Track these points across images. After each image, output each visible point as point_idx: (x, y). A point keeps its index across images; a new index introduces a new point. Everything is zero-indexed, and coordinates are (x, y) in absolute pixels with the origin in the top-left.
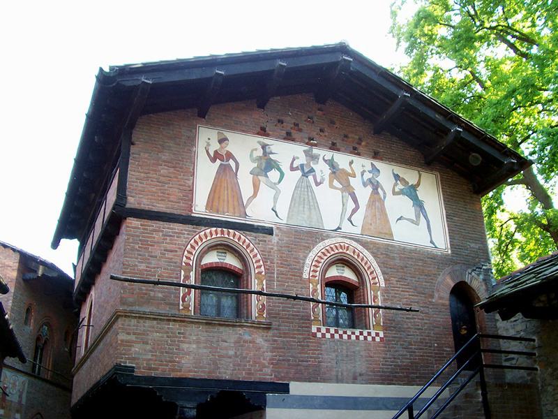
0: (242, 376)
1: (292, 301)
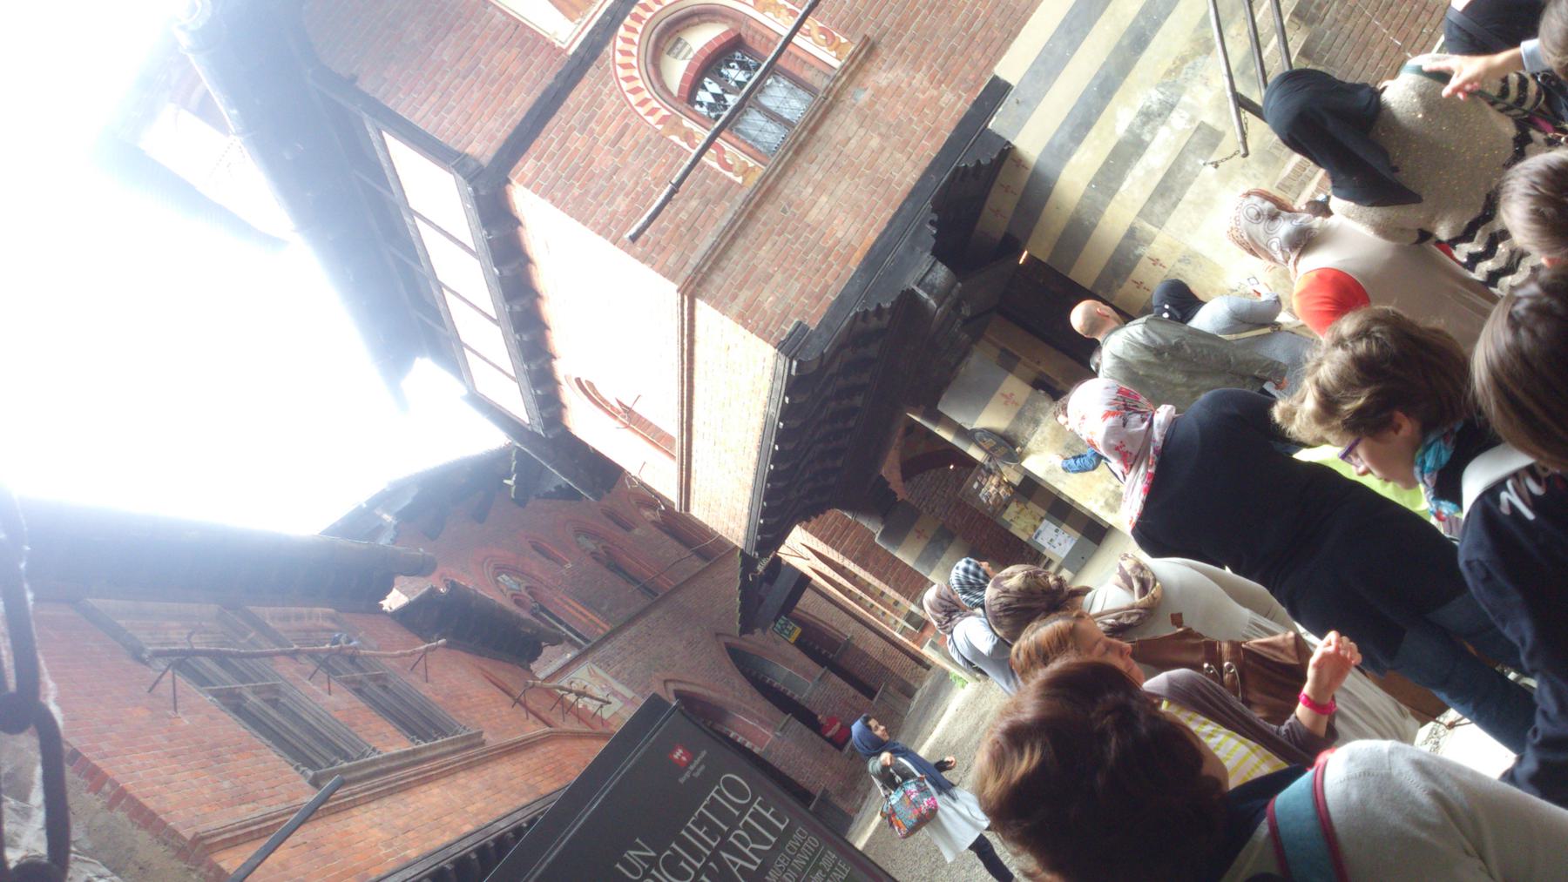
0: (930, 149)
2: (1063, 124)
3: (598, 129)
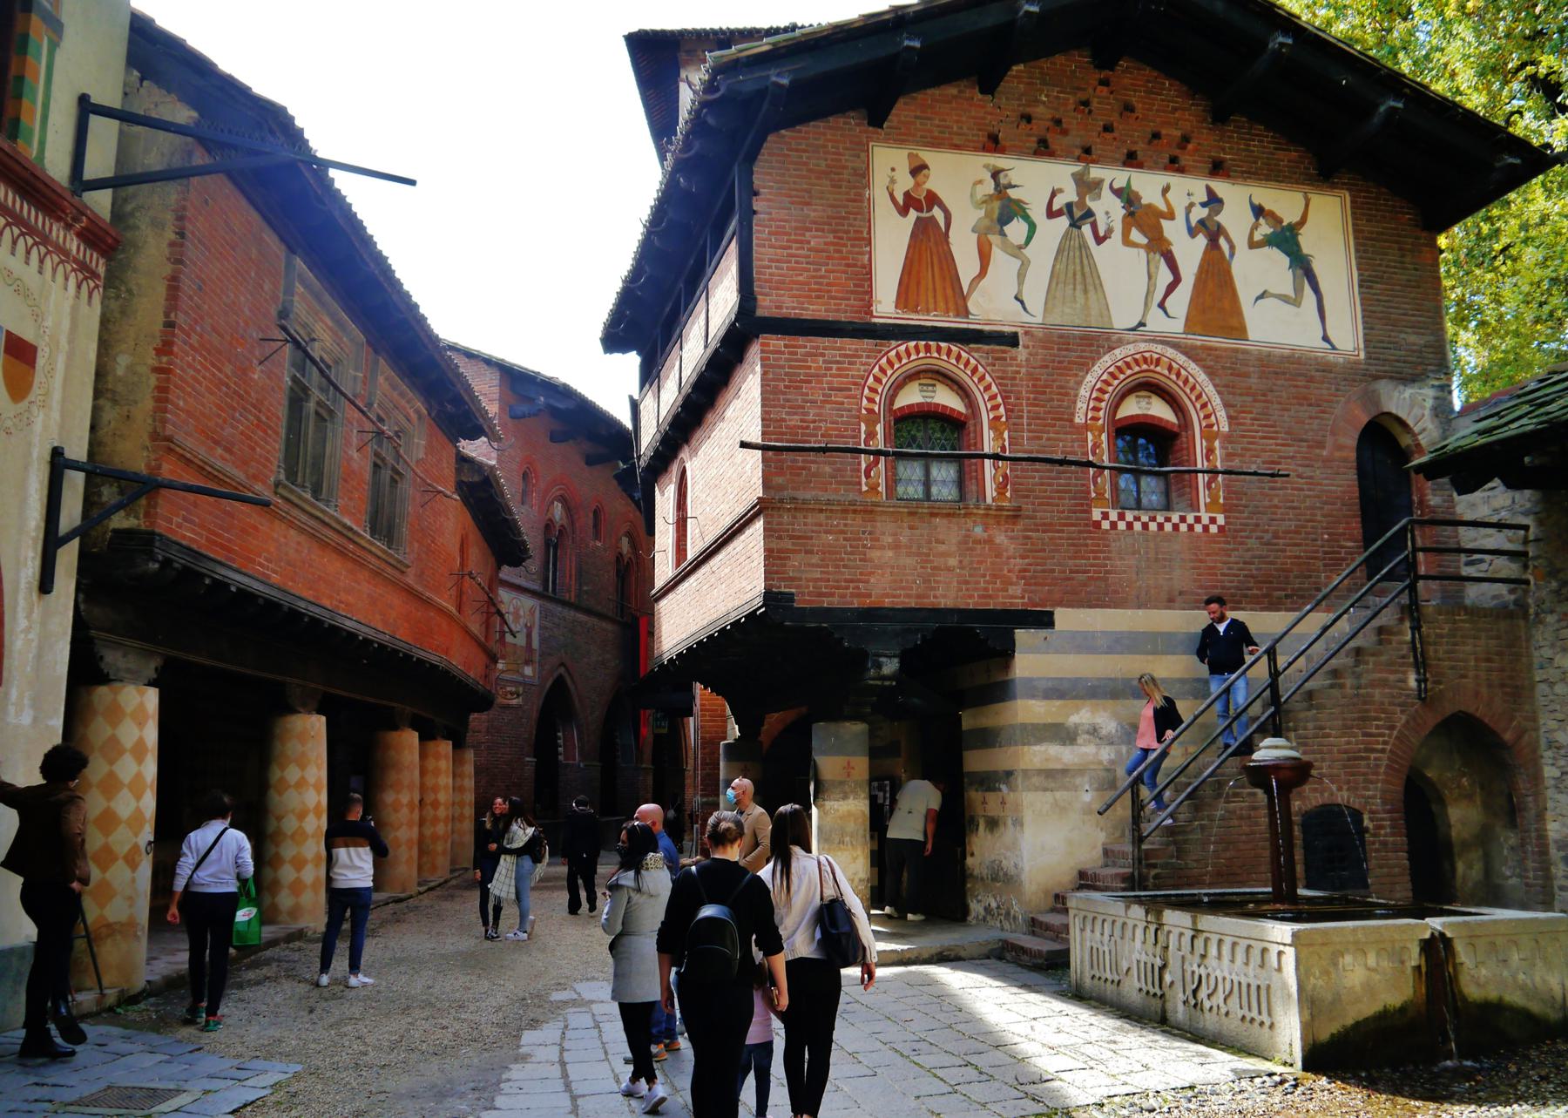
1: (1057, 467)
2: (1049, 679)
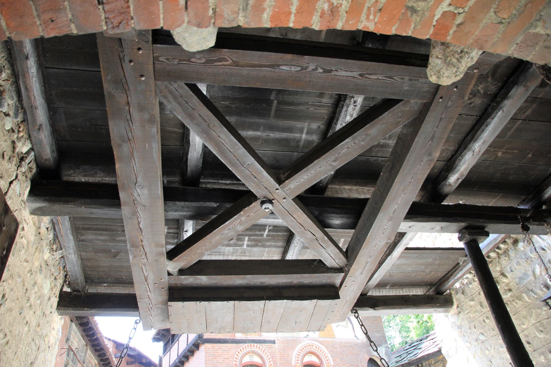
3: (225, 353)
